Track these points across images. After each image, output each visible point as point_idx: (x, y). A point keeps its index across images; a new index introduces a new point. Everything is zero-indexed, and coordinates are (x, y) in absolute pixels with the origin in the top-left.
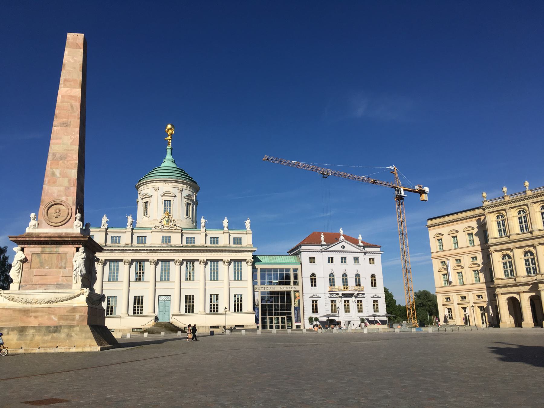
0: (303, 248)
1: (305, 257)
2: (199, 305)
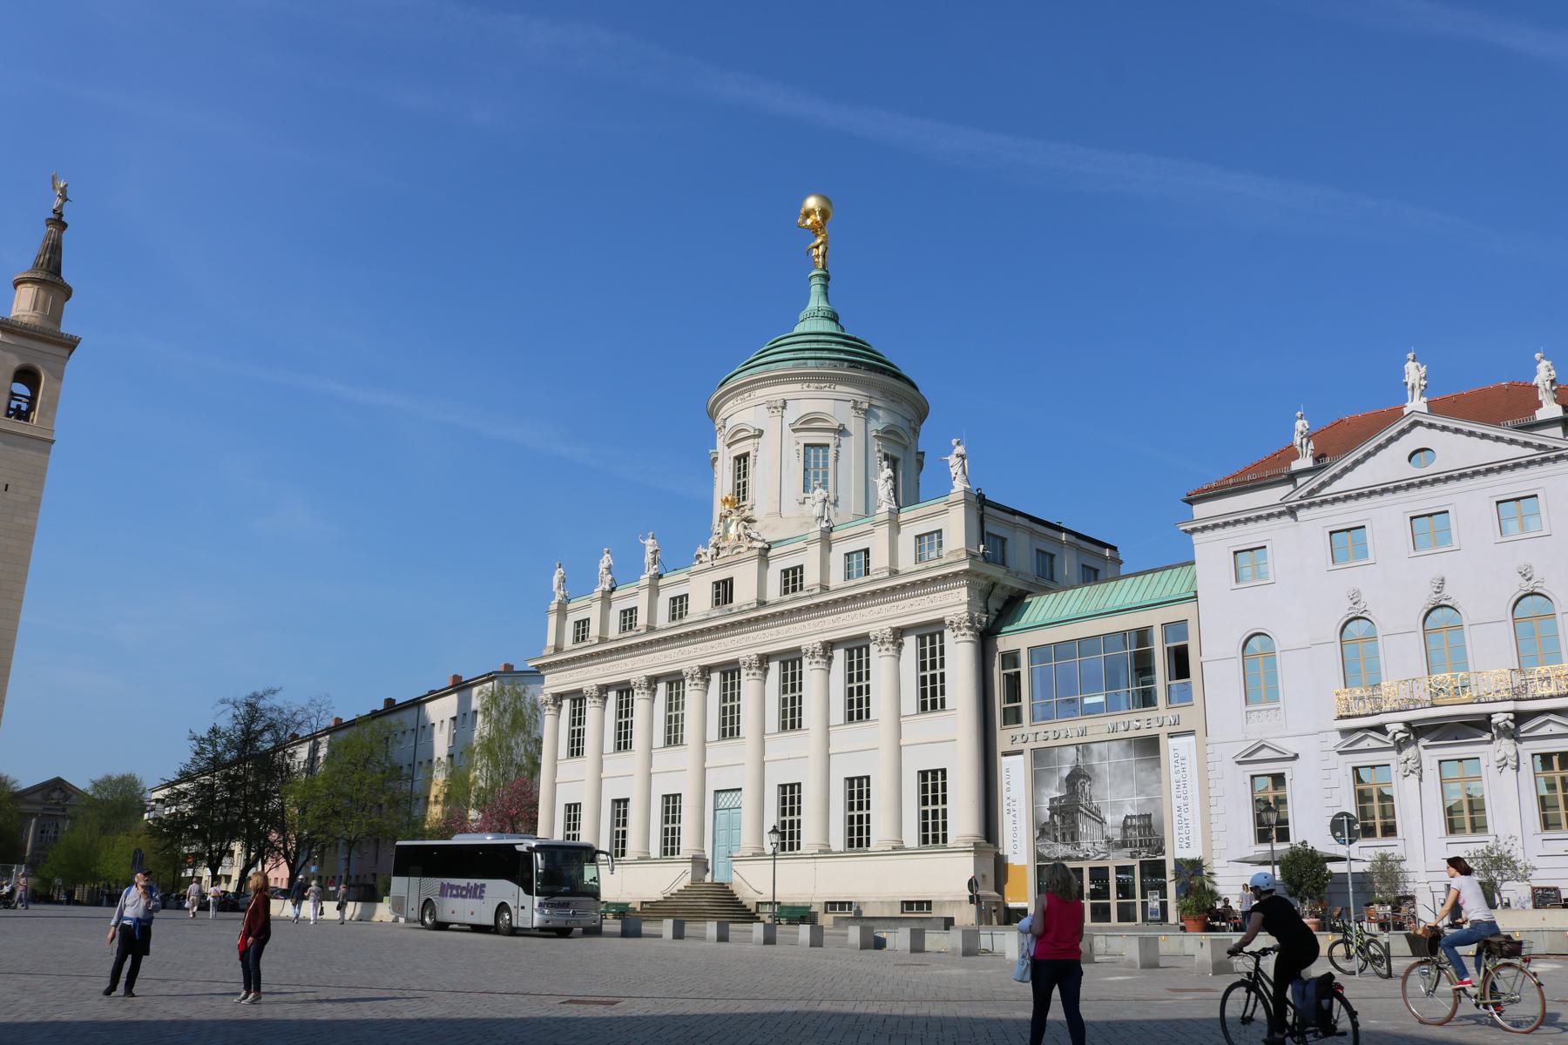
0: (1202, 510)
2: (821, 819)
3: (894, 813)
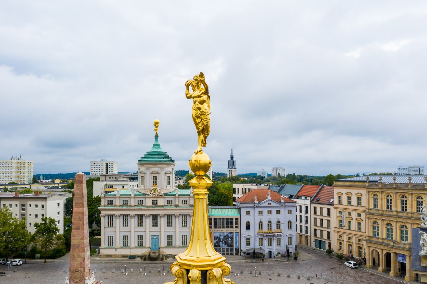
1: (243, 211)
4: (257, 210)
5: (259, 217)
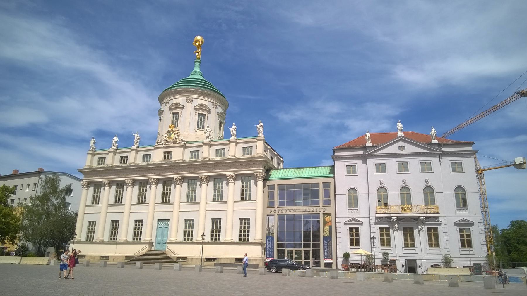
1: (341, 166)
3: (230, 231)
4: (372, 162)
5: (375, 179)
